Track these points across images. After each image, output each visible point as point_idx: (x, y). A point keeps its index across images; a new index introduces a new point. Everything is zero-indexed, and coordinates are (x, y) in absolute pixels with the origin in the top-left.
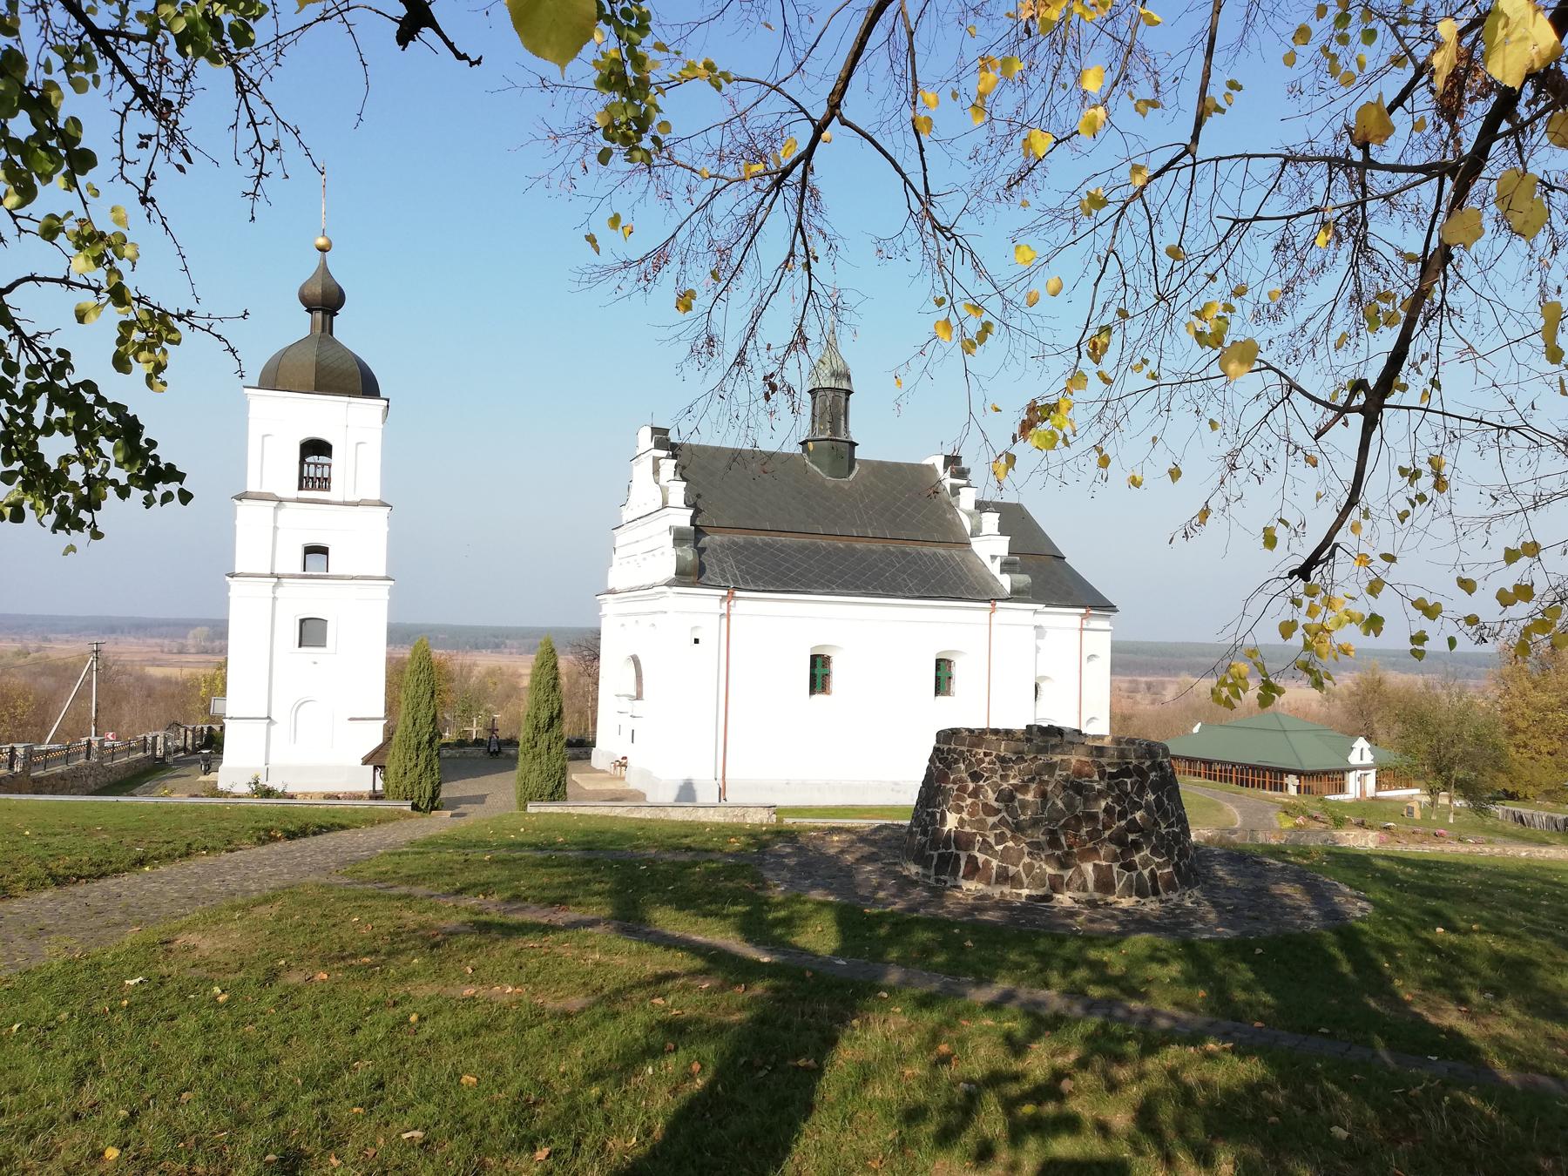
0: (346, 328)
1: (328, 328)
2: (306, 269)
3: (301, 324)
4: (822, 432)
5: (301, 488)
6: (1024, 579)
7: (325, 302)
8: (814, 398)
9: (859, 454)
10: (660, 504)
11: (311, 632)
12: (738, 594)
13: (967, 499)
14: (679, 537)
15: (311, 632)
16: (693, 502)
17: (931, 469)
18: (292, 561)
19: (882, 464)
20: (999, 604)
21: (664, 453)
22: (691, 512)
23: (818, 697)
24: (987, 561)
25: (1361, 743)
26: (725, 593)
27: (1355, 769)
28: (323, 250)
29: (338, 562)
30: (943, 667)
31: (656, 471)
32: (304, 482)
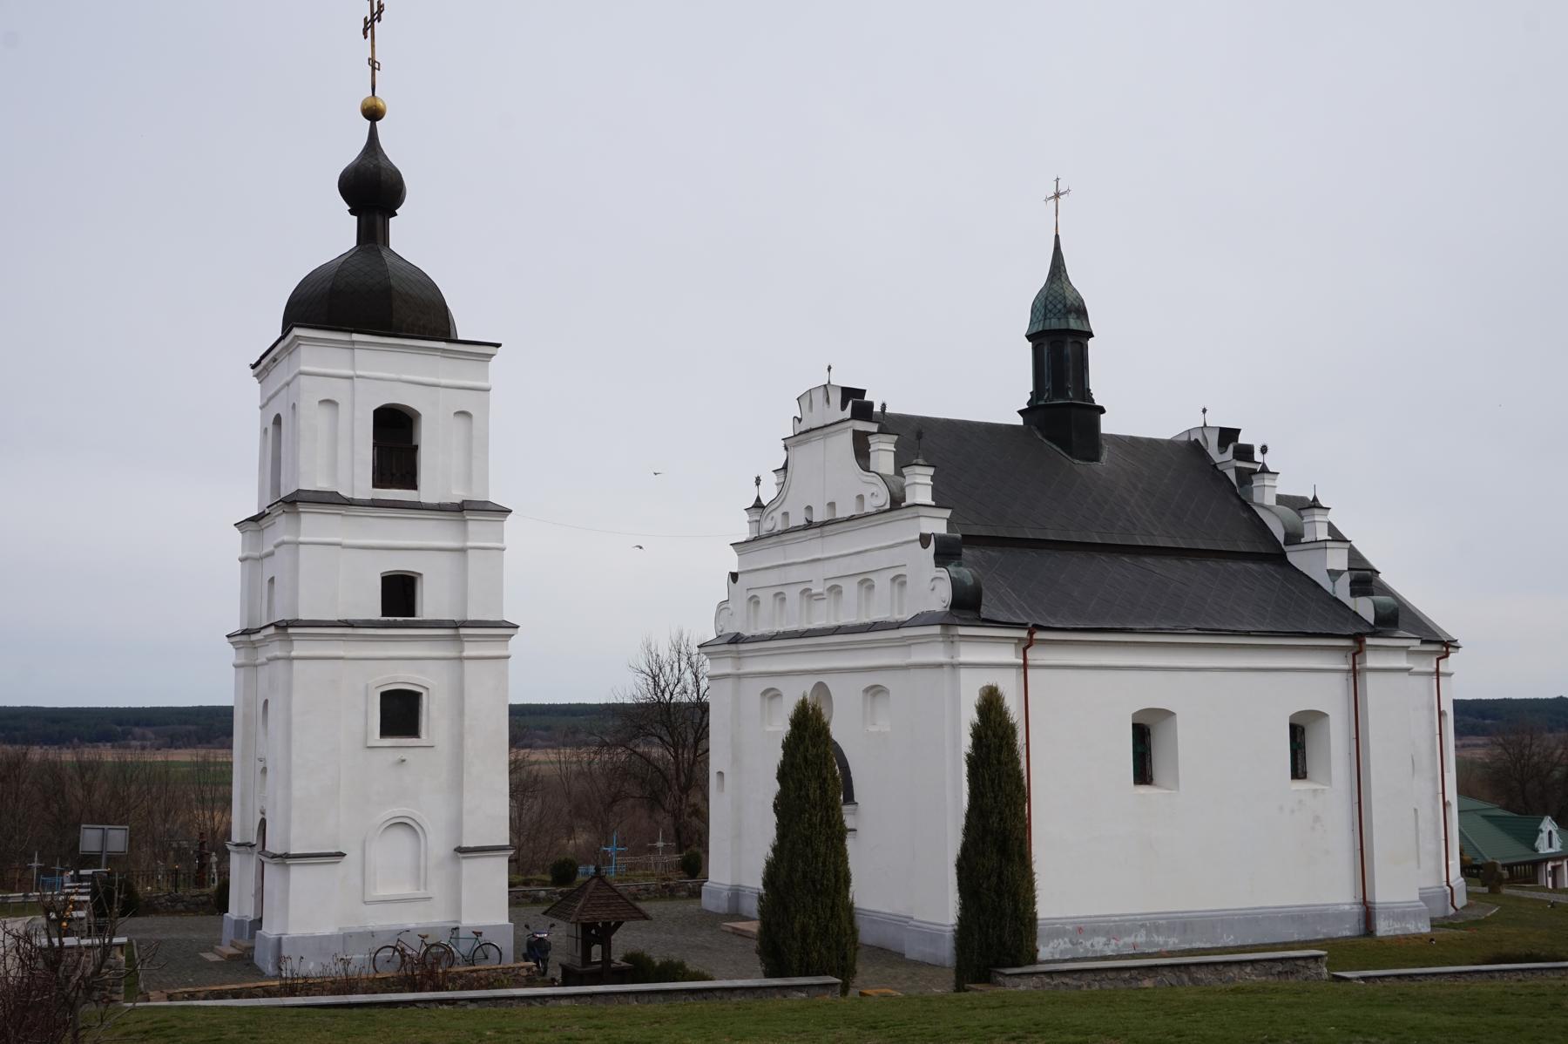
0: (407, 236)
2: (350, 151)
4: (1059, 390)
5: (374, 486)
9: (1108, 425)
10: (883, 499)
11: (401, 714)
12: (1038, 635)
13: (1266, 494)
14: (946, 552)
15: (401, 714)
16: (941, 499)
20: (1369, 641)
21: (874, 428)
22: (947, 513)
23: (1143, 790)
24: (1326, 583)
25: (1548, 825)
26: (1024, 634)
27: (1546, 859)
29: (430, 603)
30: (1297, 733)
32: (380, 480)
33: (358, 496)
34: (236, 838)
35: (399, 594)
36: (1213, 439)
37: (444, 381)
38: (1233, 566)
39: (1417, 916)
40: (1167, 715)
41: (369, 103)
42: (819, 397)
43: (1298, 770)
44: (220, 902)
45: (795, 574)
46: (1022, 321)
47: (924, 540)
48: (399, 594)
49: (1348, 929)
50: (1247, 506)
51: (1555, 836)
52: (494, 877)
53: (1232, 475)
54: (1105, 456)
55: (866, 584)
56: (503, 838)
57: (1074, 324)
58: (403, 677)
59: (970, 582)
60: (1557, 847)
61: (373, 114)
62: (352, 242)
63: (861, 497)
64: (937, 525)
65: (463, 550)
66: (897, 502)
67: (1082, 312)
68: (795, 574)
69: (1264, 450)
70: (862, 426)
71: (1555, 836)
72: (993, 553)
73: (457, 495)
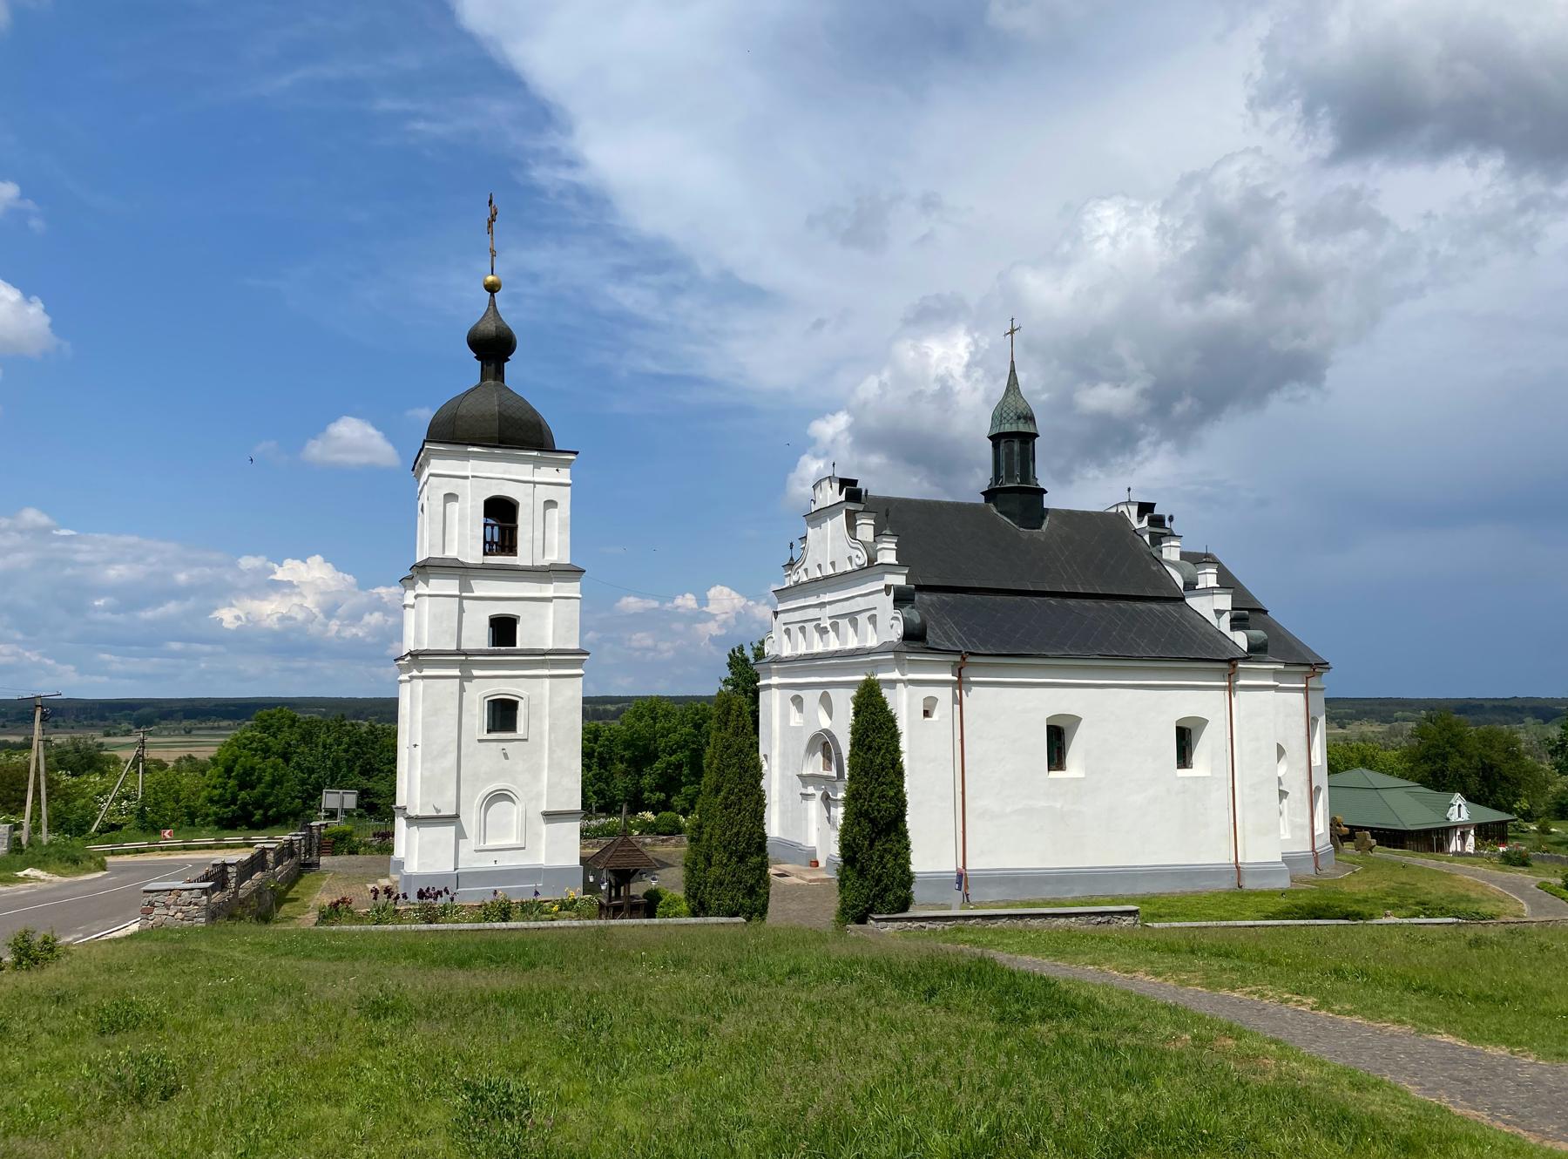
1: (499, 375)
3: (470, 369)
4: (1010, 477)
5: (485, 554)
6: (1258, 633)
7: (493, 348)
8: (996, 446)
9: (1049, 502)
10: (863, 559)
11: (503, 714)
13: (1171, 552)
14: (901, 598)
15: (503, 714)
17: (1121, 518)
18: (478, 636)
19: (1070, 513)
21: (860, 507)
25: (1458, 799)
26: (958, 658)
28: (492, 289)
31: (851, 526)
32: (489, 548)
33: (470, 561)
34: (398, 804)
35: (504, 629)
36: (1134, 510)
37: (537, 479)
38: (1139, 605)
39: (1277, 873)
40: (1076, 720)
41: (490, 278)
42: (826, 484)
43: (1184, 756)
44: (390, 850)
45: (812, 613)
46: (986, 427)
47: (887, 588)
48: (504, 629)
49: (1227, 884)
50: (1159, 561)
51: (1463, 808)
52: (571, 831)
53: (1147, 538)
54: (1044, 527)
55: (854, 624)
56: (577, 805)
57: (1022, 427)
58: (504, 688)
59: (917, 620)
60: (1465, 816)
61: (492, 289)
62: (475, 378)
63: (850, 558)
64: (900, 580)
65: (549, 600)
66: (871, 560)
67: (1030, 418)
68: (812, 613)
69: (1171, 519)
70: (852, 506)
71: (1463, 808)
72: (946, 597)
73: (541, 562)
